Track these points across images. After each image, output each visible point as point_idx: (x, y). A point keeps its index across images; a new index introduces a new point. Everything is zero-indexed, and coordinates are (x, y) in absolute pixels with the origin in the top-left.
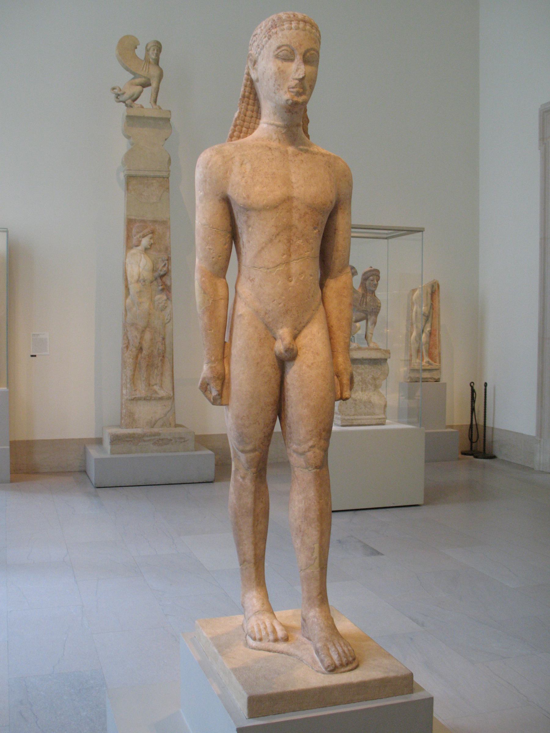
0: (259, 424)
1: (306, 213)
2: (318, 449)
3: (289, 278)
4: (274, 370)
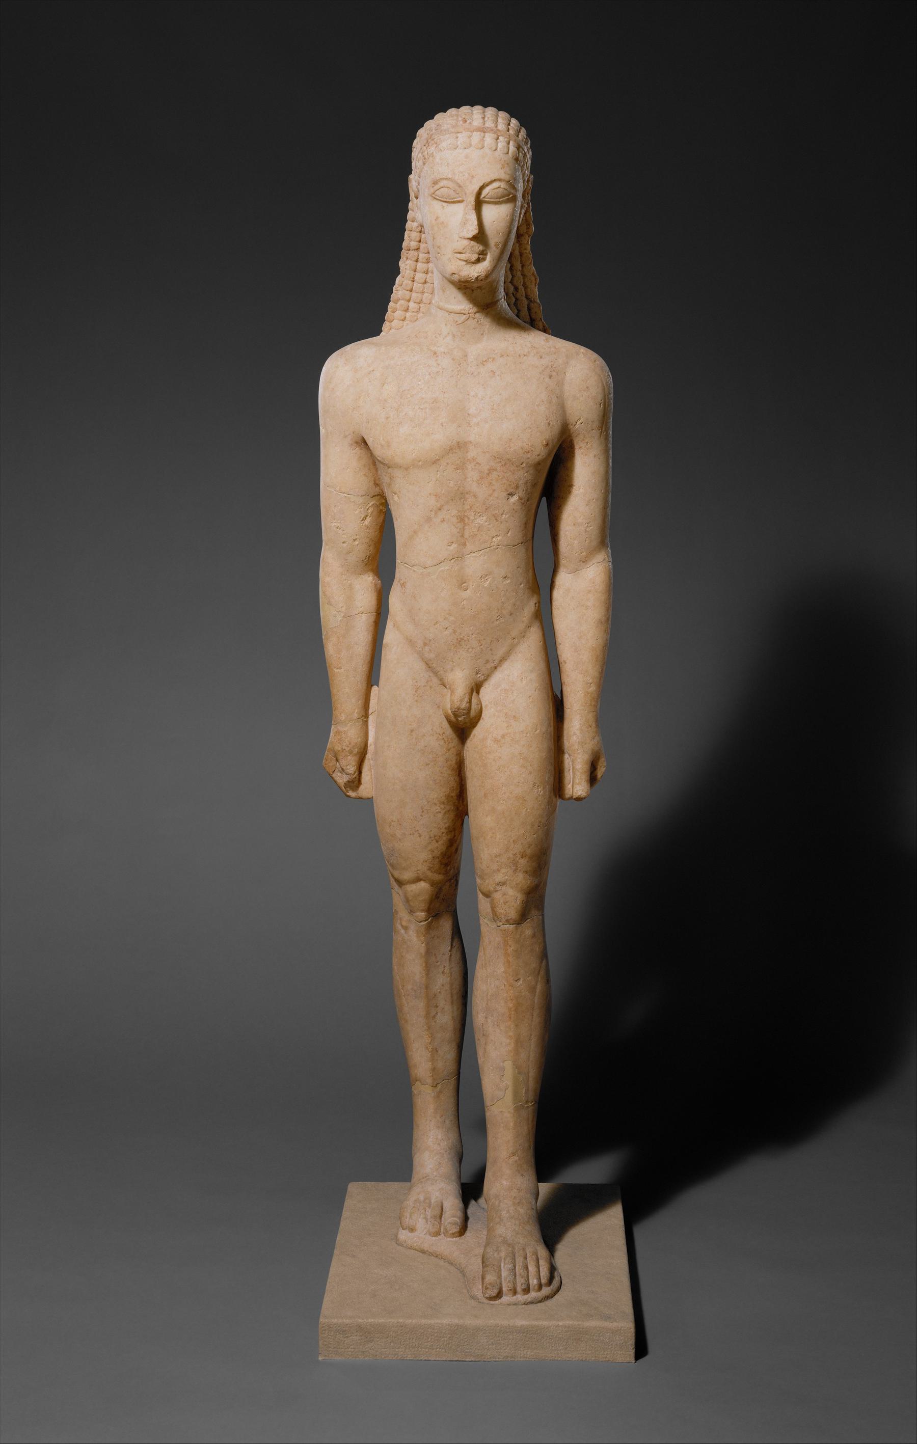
0: (420, 836)
1: (491, 470)
2: (512, 888)
3: (462, 584)
4: (442, 742)
